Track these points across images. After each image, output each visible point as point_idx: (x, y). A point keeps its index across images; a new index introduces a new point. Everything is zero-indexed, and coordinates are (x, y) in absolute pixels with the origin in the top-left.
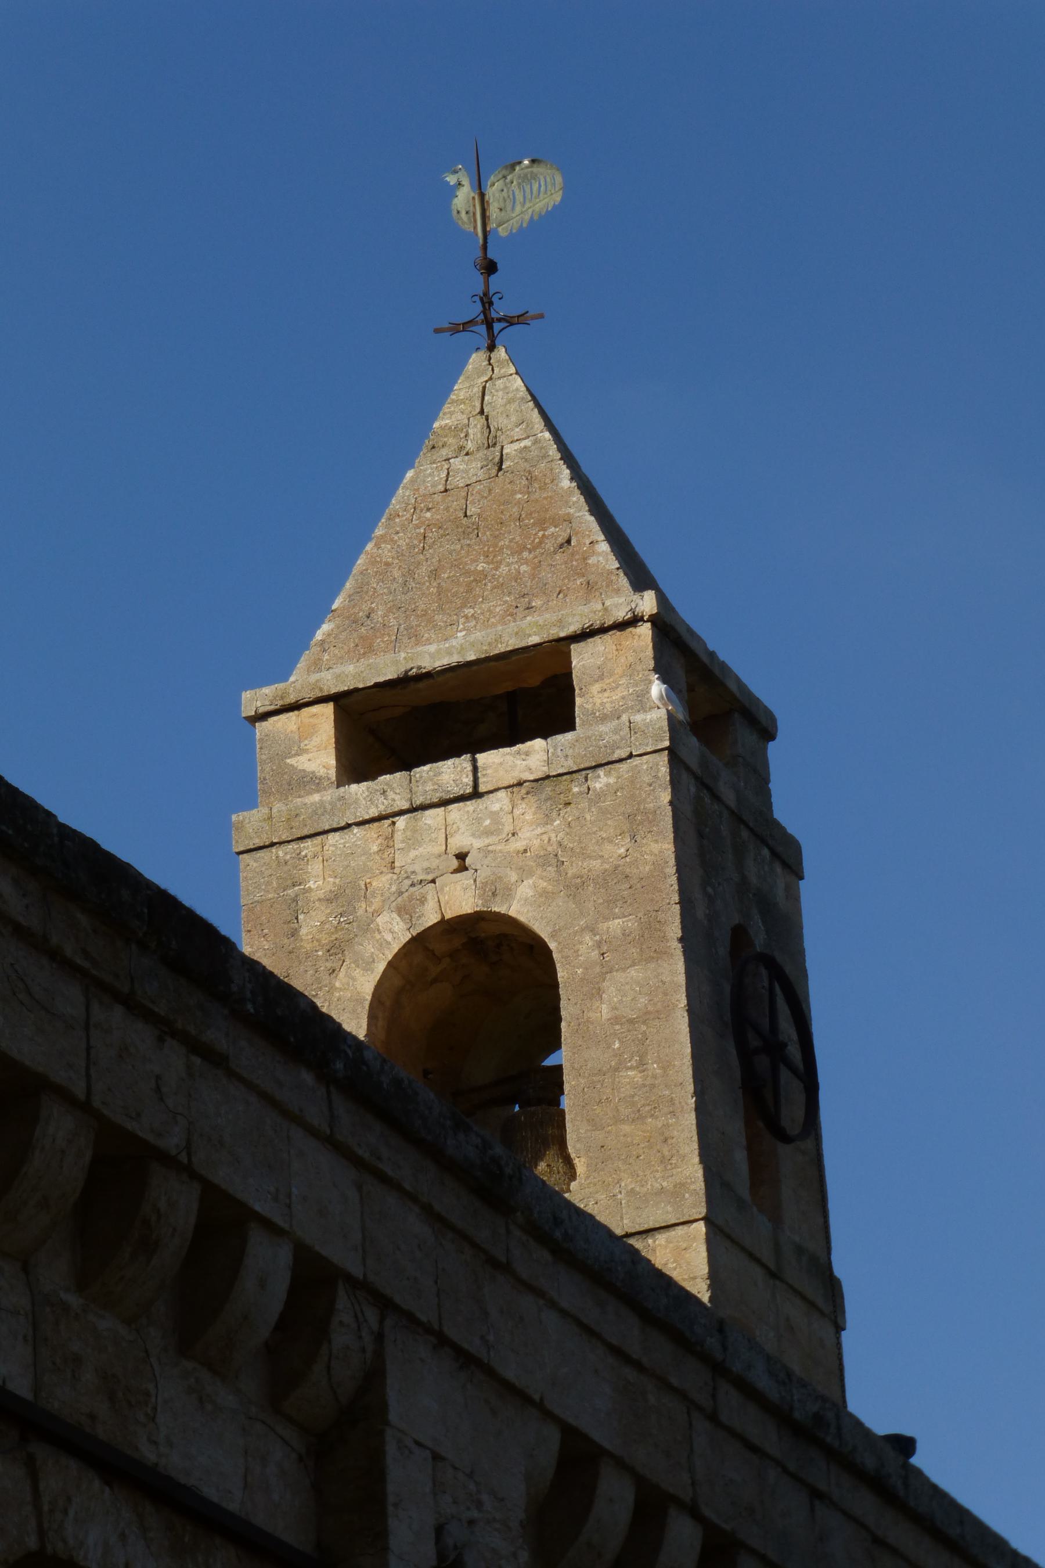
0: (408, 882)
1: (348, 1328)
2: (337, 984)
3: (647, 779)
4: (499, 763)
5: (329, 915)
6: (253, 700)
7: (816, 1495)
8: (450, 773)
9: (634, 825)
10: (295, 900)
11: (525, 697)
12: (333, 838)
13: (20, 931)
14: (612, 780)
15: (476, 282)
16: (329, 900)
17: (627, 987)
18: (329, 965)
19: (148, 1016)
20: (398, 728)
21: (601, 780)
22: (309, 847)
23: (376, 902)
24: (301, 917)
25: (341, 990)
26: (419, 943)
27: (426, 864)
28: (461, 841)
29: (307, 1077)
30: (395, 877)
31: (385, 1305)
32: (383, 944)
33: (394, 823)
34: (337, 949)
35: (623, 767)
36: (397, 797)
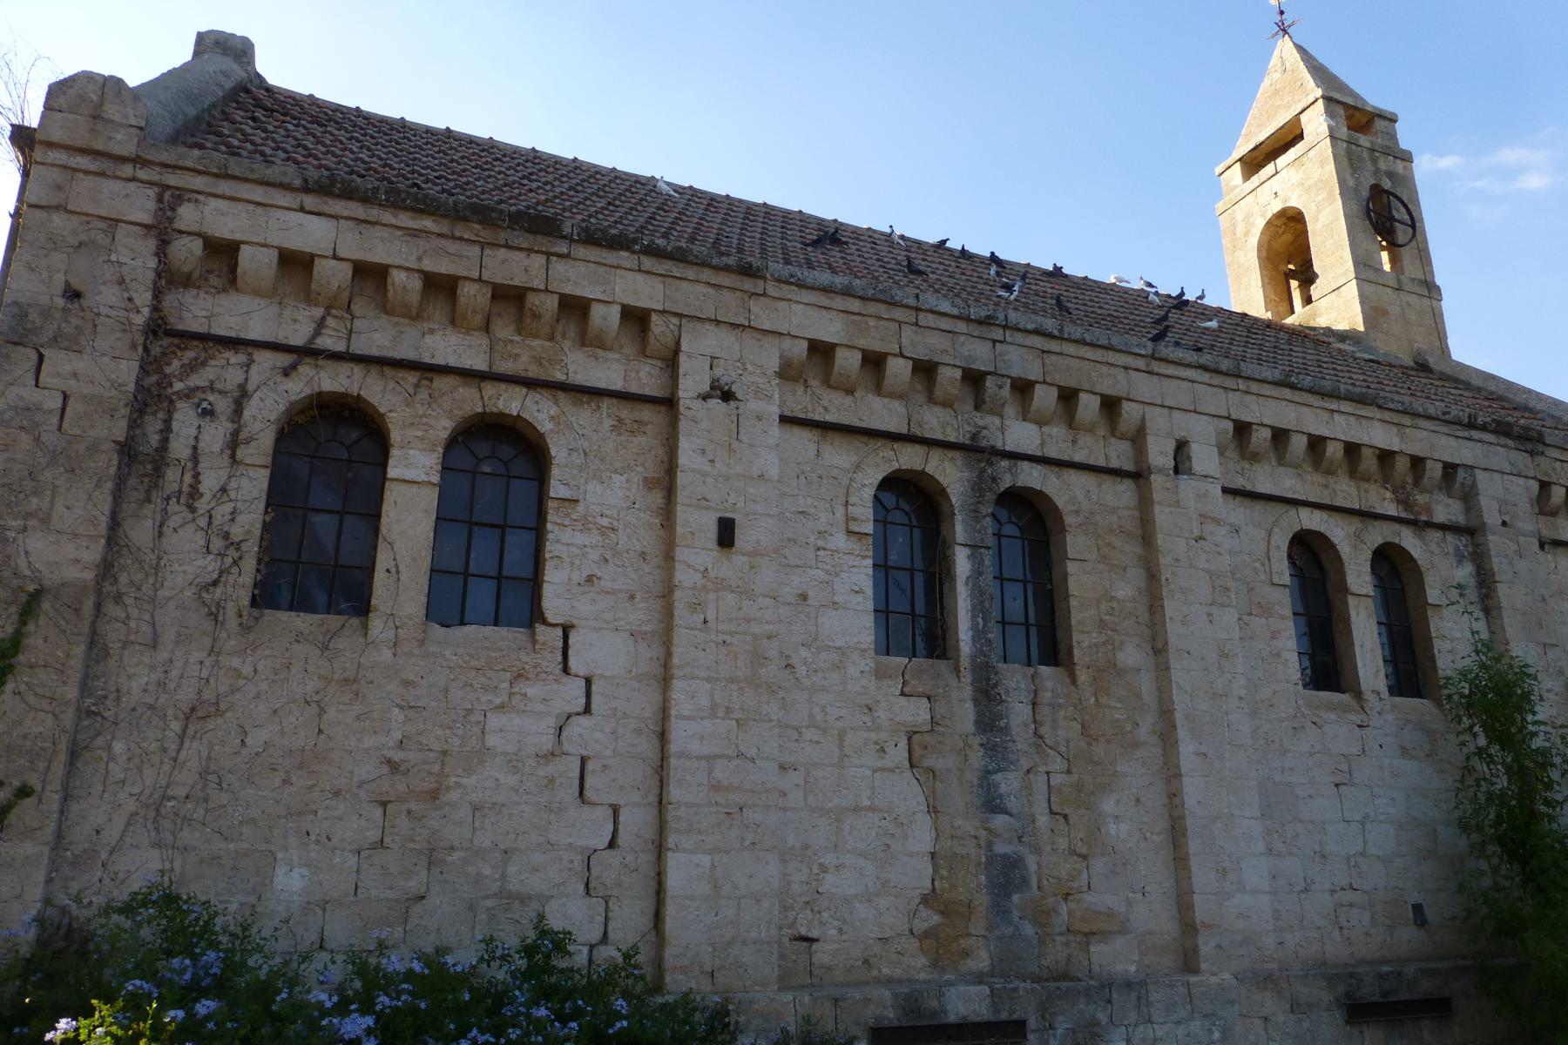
1: (658, 325)
4: (1282, 161)
6: (1218, 170)
7: (995, 341)
8: (1269, 169)
9: (1322, 164)
11: (1289, 137)
13: (440, 235)
15: (1278, 18)
19: (521, 249)
20: (1255, 161)
26: (1269, 223)
29: (624, 254)
31: (680, 315)
34: (1246, 234)
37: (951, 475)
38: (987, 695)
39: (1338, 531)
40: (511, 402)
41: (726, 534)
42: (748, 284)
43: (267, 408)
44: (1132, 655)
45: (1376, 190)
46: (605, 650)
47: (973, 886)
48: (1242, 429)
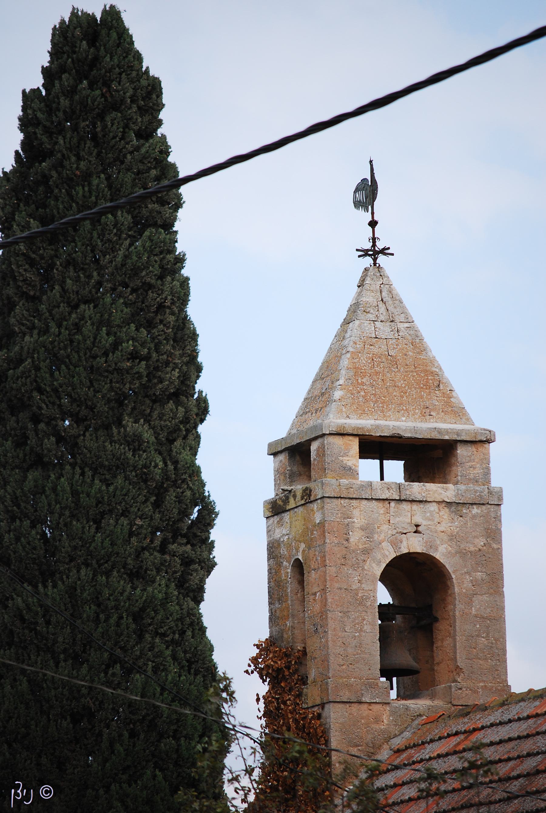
0: (396, 531)
2: (366, 568)
3: (493, 515)
5: (363, 536)
10: (348, 525)
12: (364, 502)
14: (479, 512)
16: (362, 529)
17: (483, 603)
18: (362, 558)
21: (475, 510)
22: (354, 503)
23: (382, 536)
24: (351, 533)
25: (367, 570)
27: (403, 525)
28: (418, 519)
30: (390, 527)
32: (385, 556)
33: (389, 503)
35: (484, 507)
36: (394, 493)
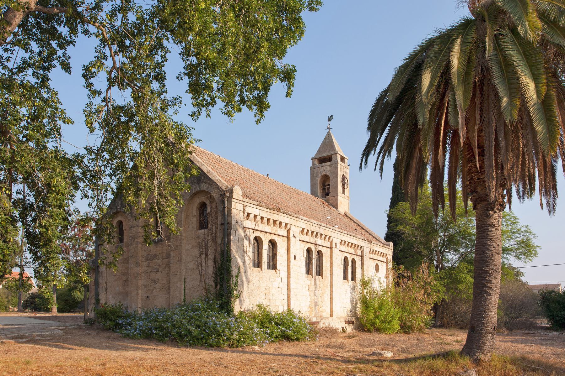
37: (313, 247)
38: (315, 280)
39: (348, 256)
40: (274, 237)
41: (295, 257)
42: (297, 219)
43: (252, 238)
44: (328, 275)
45: (343, 175)
46: (284, 274)
47: (313, 305)
48: (342, 241)
